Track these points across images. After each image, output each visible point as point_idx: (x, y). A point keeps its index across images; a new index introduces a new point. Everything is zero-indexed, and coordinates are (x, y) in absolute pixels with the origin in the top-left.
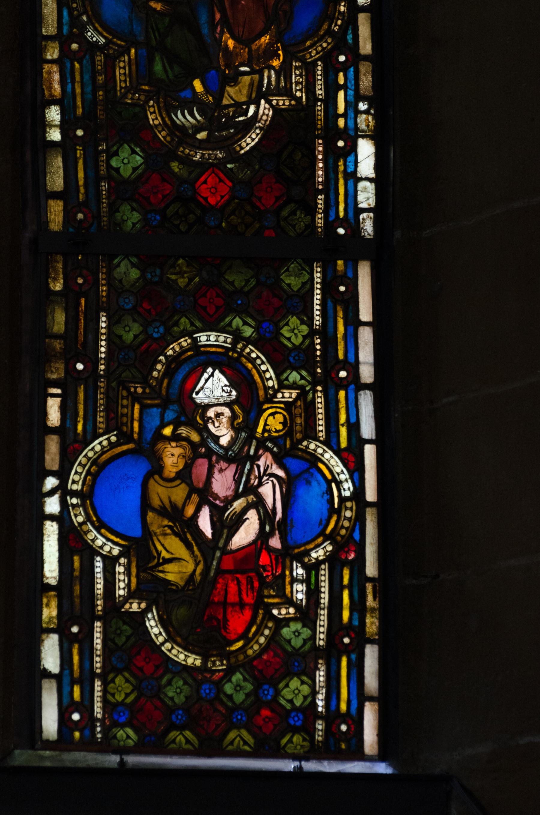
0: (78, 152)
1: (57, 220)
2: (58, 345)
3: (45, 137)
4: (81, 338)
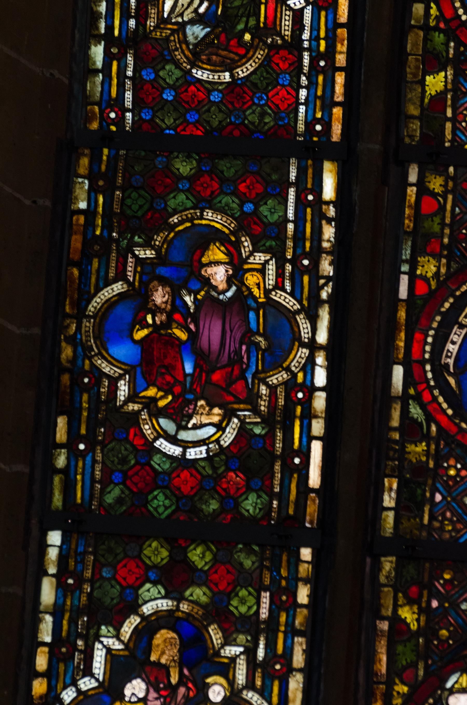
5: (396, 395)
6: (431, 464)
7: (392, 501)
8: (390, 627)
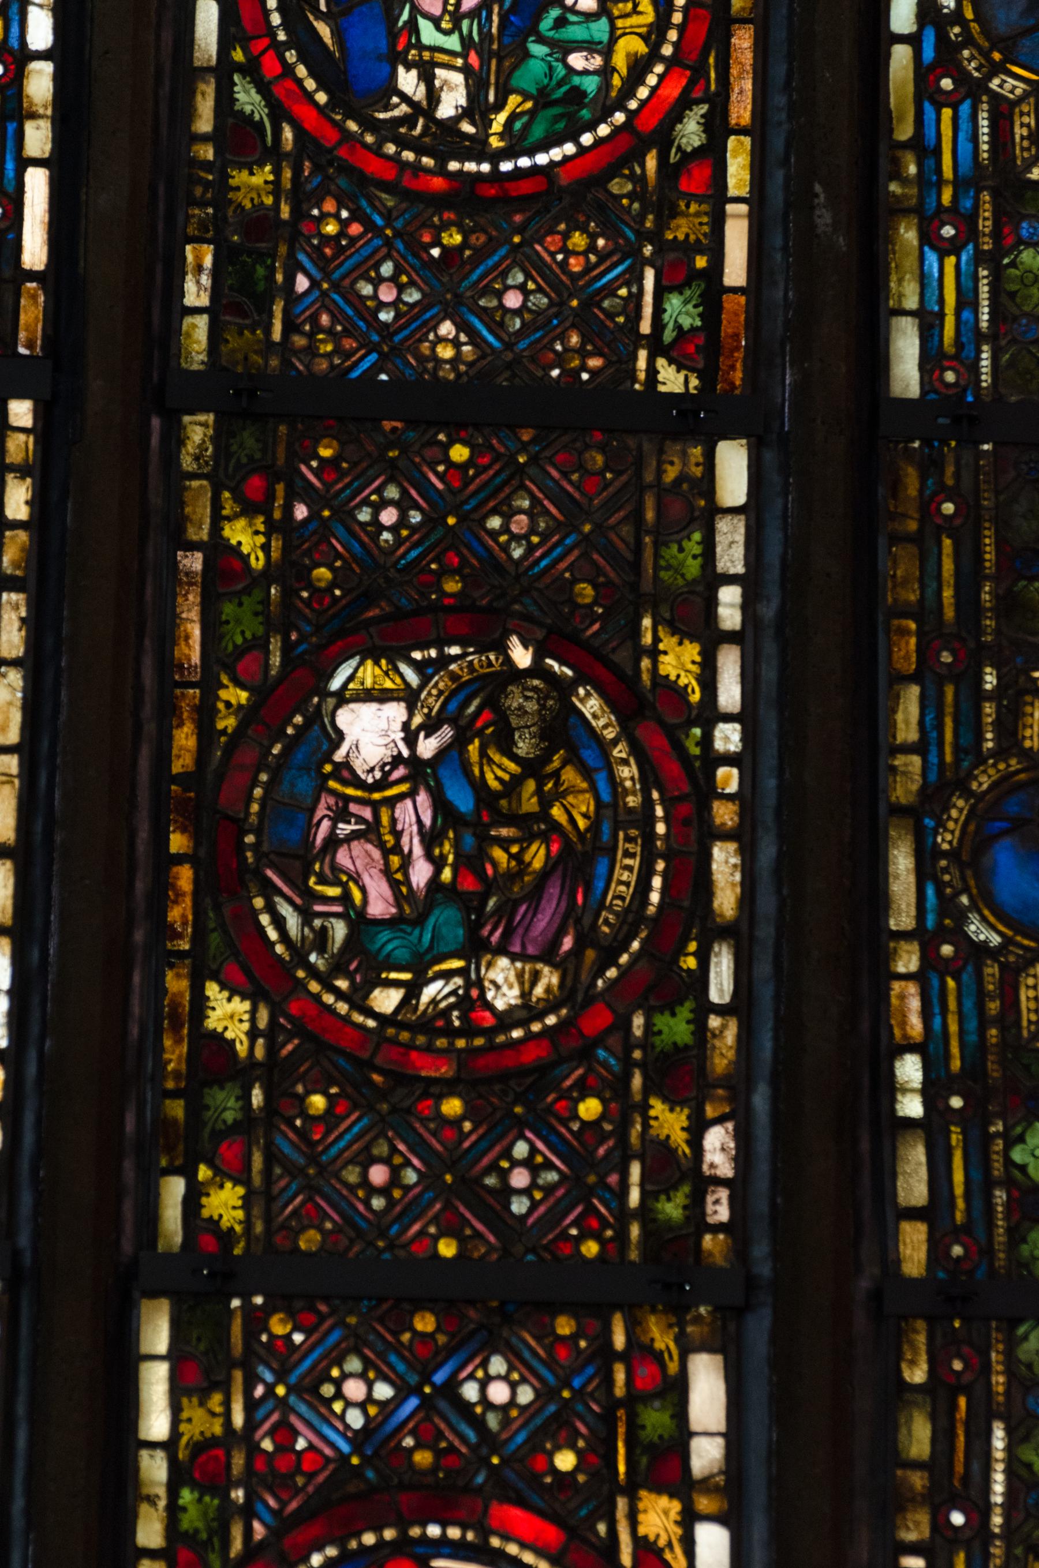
0: (954, 1137)
1: (916, 1258)
2: (918, 1480)
3: (893, 1110)
4: (959, 1468)
5: (205, 65)
6: (285, 212)
7: (202, 293)
8: (206, 563)
